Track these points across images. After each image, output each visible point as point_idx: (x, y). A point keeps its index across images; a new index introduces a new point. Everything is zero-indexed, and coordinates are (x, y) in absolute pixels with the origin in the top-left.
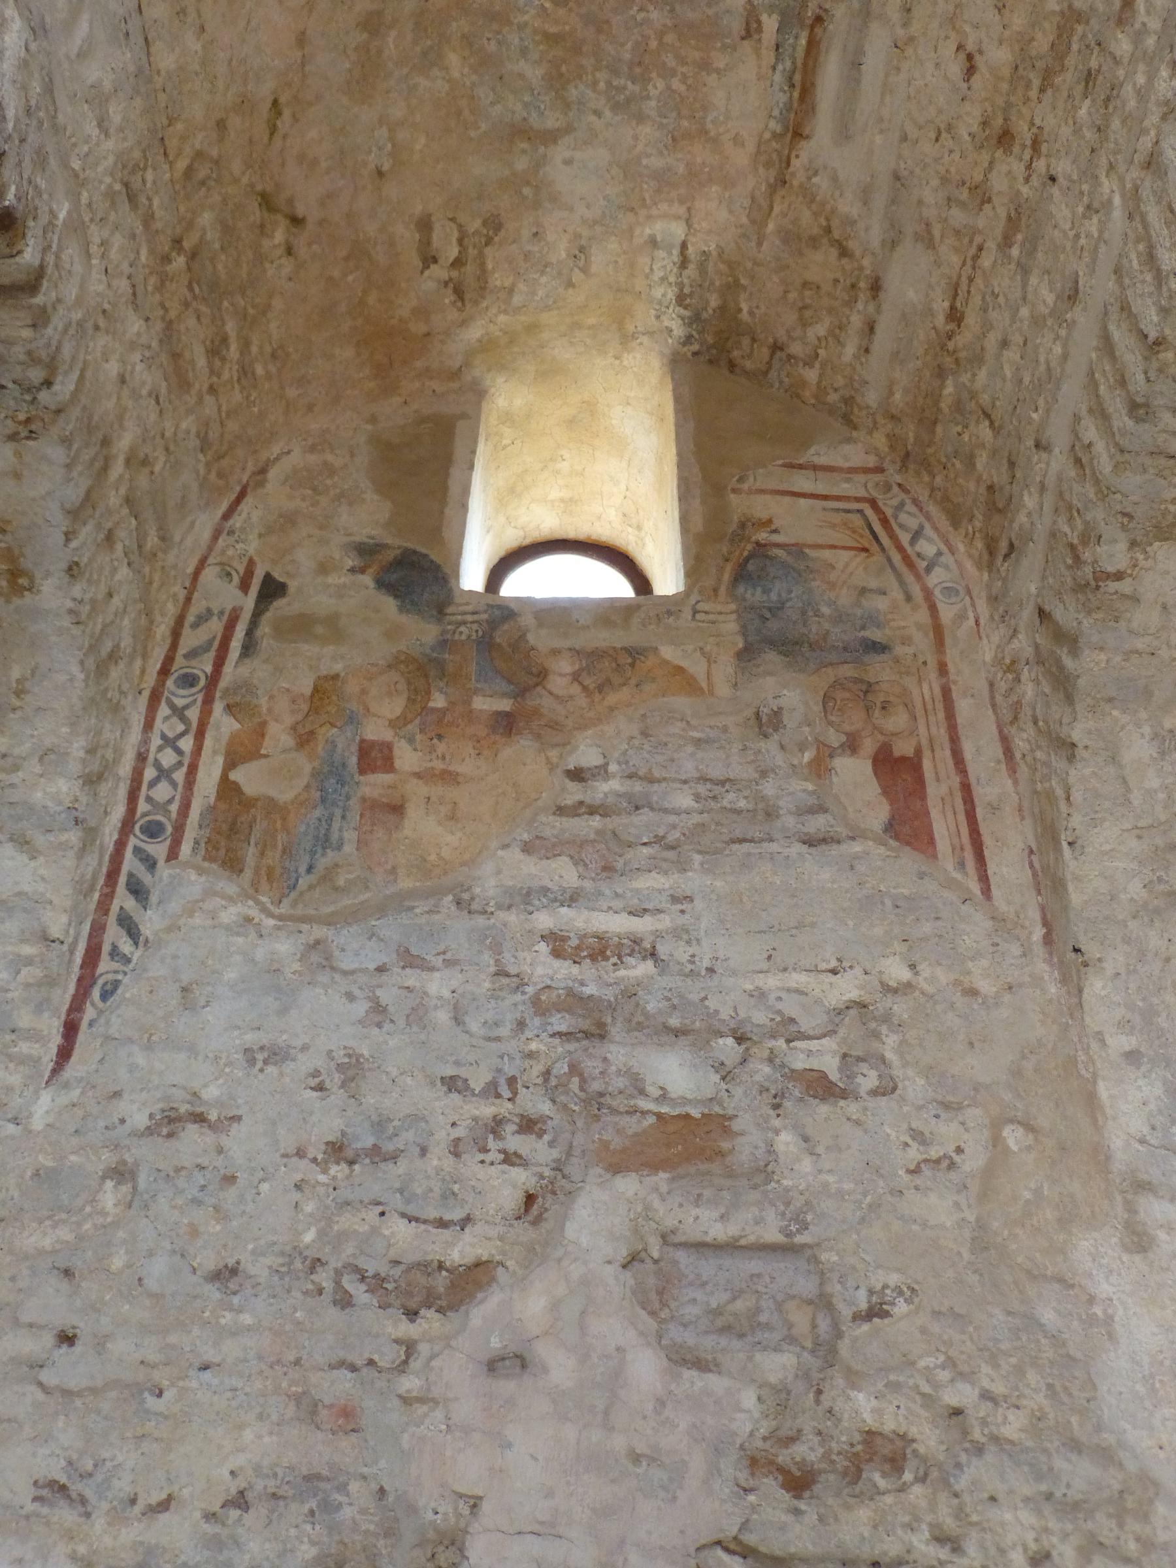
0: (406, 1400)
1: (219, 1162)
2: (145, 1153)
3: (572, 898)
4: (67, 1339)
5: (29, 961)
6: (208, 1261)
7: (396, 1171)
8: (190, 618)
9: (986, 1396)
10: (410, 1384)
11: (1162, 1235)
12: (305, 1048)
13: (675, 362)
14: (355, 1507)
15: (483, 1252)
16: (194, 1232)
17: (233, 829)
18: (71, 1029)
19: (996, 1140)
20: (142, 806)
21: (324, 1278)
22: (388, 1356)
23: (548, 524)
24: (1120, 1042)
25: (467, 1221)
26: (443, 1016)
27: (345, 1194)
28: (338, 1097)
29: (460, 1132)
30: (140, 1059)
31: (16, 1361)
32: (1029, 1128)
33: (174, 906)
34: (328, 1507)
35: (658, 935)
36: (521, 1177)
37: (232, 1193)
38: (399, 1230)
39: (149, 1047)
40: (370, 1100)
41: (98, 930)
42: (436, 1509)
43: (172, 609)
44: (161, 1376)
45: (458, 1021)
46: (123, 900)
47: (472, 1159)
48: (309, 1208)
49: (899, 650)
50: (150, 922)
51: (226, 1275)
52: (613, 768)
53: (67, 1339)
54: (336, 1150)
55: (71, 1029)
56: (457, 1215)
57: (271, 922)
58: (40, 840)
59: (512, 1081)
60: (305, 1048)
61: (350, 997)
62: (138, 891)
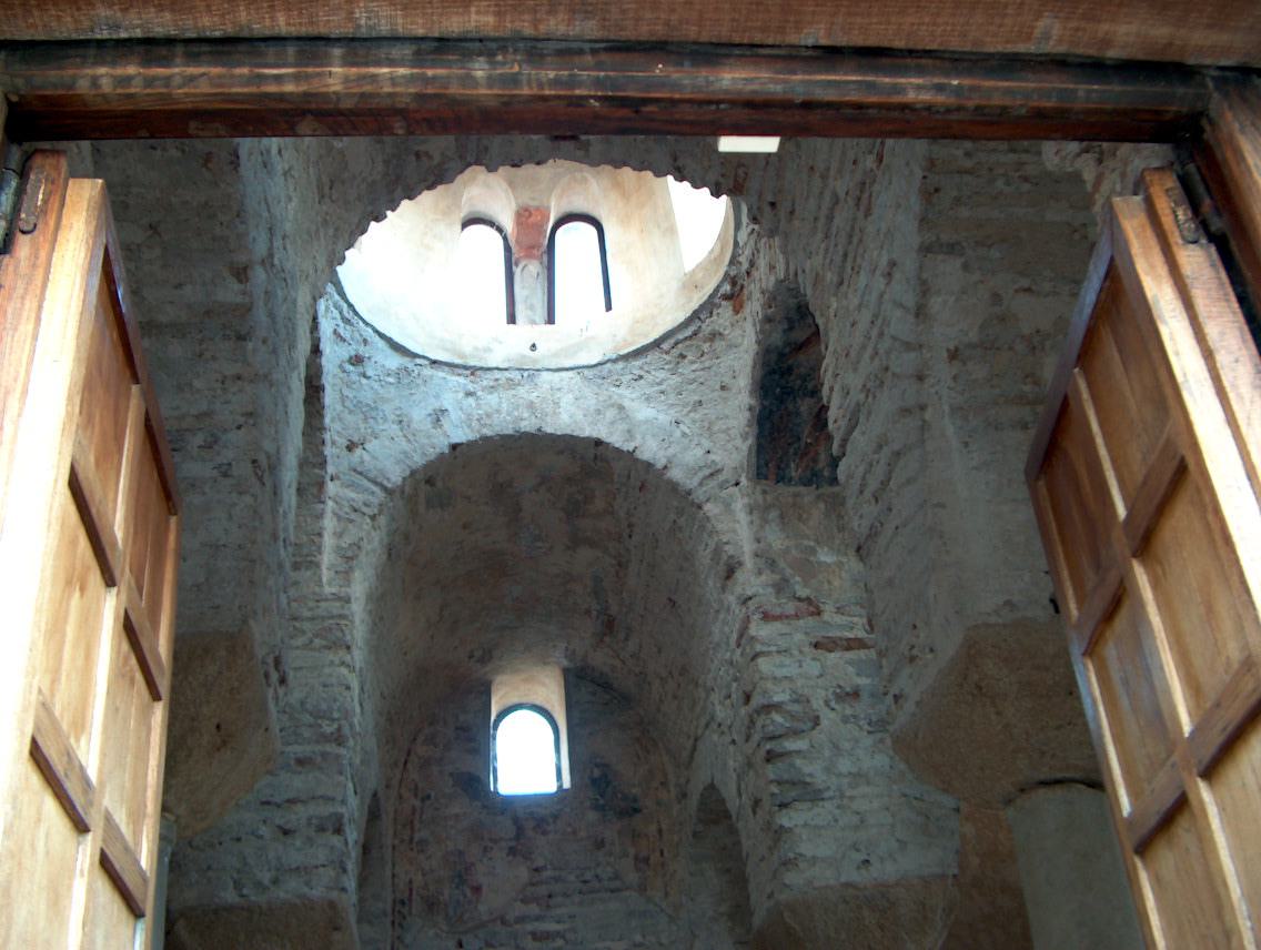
3: (538, 918)
13: (566, 672)
23: (515, 700)
35: (565, 931)
49: (645, 811)
52: (549, 867)
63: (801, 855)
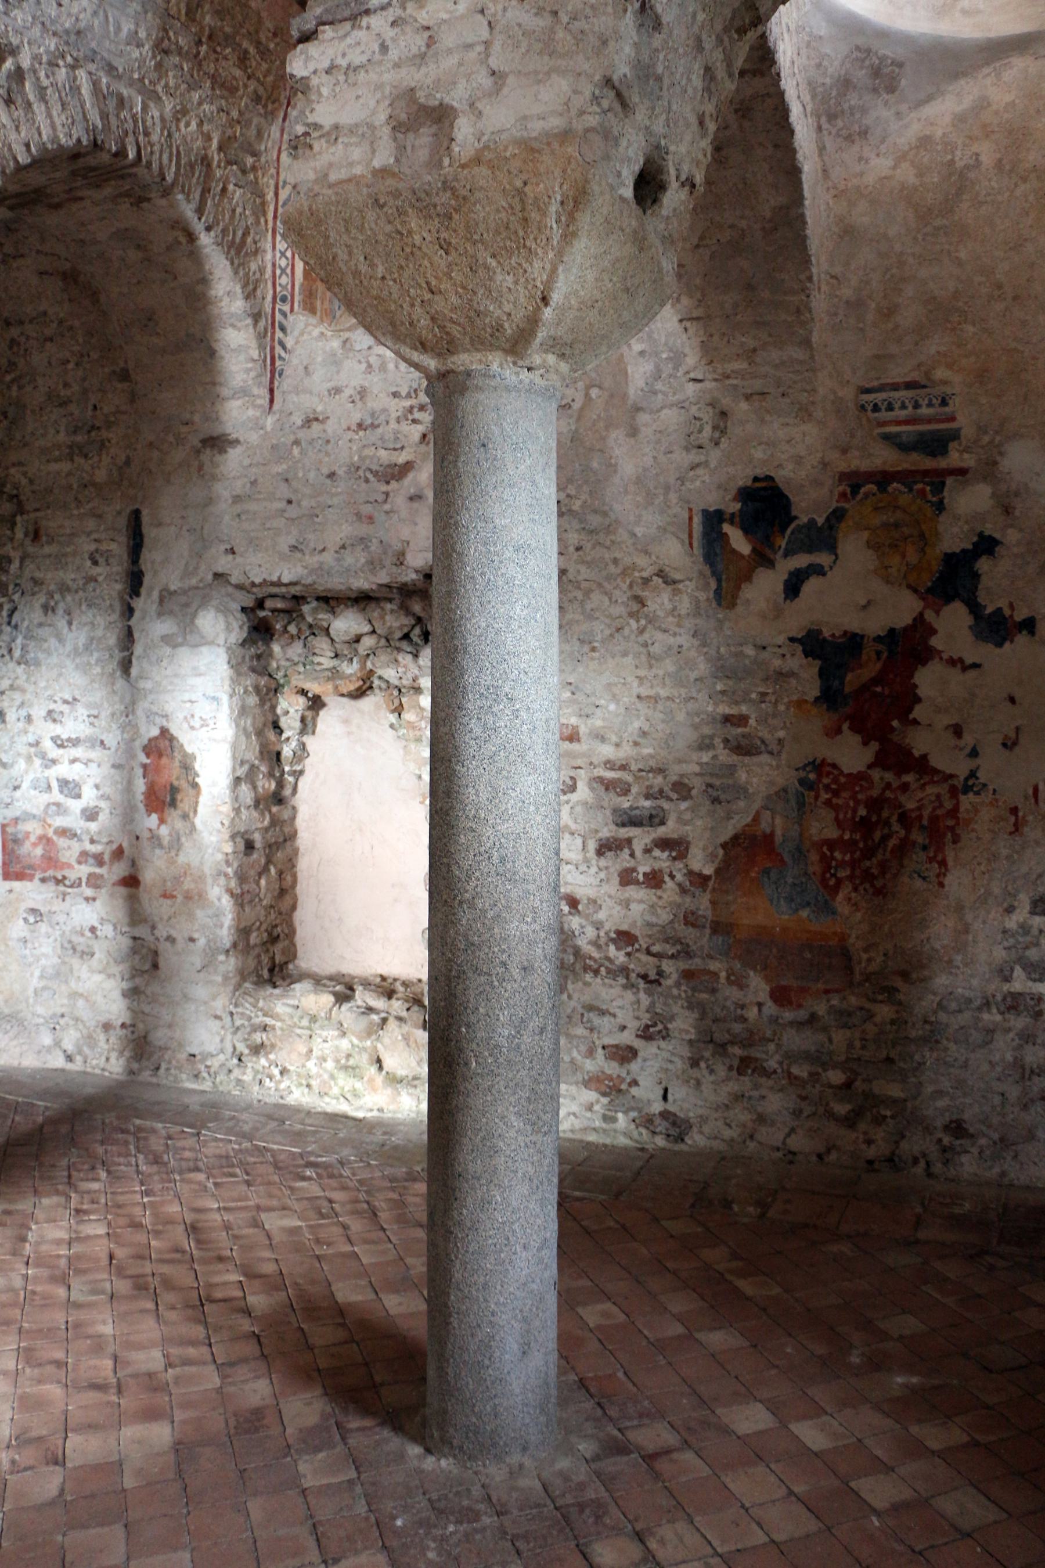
0: (387, 513)
2: (301, 435)
4: (290, 502)
5: (251, 369)
6: (325, 471)
7: (380, 430)
8: (281, 184)
9: (568, 496)
10: (387, 507)
11: (643, 429)
14: (374, 546)
15: (409, 458)
16: (321, 462)
17: (311, 294)
18: (271, 391)
20: (278, 289)
21: (361, 473)
22: (381, 498)
25: (402, 448)
27: (364, 442)
28: (359, 404)
31: (277, 510)
32: (600, 387)
33: (296, 333)
34: (367, 547)
36: (420, 429)
37: (330, 447)
38: (382, 453)
39: (297, 394)
41: (272, 349)
42: (397, 546)
43: (272, 182)
44: (317, 511)
46: (279, 334)
47: (404, 423)
50: (289, 342)
51: (332, 475)
53: (290, 502)
54: (360, 426)
55: (271, 391)
56: (398, 446)
58: (239, 324)
59: (416, 391)
61: (360, 362)
62: (283, 329)
63: (316, 126)
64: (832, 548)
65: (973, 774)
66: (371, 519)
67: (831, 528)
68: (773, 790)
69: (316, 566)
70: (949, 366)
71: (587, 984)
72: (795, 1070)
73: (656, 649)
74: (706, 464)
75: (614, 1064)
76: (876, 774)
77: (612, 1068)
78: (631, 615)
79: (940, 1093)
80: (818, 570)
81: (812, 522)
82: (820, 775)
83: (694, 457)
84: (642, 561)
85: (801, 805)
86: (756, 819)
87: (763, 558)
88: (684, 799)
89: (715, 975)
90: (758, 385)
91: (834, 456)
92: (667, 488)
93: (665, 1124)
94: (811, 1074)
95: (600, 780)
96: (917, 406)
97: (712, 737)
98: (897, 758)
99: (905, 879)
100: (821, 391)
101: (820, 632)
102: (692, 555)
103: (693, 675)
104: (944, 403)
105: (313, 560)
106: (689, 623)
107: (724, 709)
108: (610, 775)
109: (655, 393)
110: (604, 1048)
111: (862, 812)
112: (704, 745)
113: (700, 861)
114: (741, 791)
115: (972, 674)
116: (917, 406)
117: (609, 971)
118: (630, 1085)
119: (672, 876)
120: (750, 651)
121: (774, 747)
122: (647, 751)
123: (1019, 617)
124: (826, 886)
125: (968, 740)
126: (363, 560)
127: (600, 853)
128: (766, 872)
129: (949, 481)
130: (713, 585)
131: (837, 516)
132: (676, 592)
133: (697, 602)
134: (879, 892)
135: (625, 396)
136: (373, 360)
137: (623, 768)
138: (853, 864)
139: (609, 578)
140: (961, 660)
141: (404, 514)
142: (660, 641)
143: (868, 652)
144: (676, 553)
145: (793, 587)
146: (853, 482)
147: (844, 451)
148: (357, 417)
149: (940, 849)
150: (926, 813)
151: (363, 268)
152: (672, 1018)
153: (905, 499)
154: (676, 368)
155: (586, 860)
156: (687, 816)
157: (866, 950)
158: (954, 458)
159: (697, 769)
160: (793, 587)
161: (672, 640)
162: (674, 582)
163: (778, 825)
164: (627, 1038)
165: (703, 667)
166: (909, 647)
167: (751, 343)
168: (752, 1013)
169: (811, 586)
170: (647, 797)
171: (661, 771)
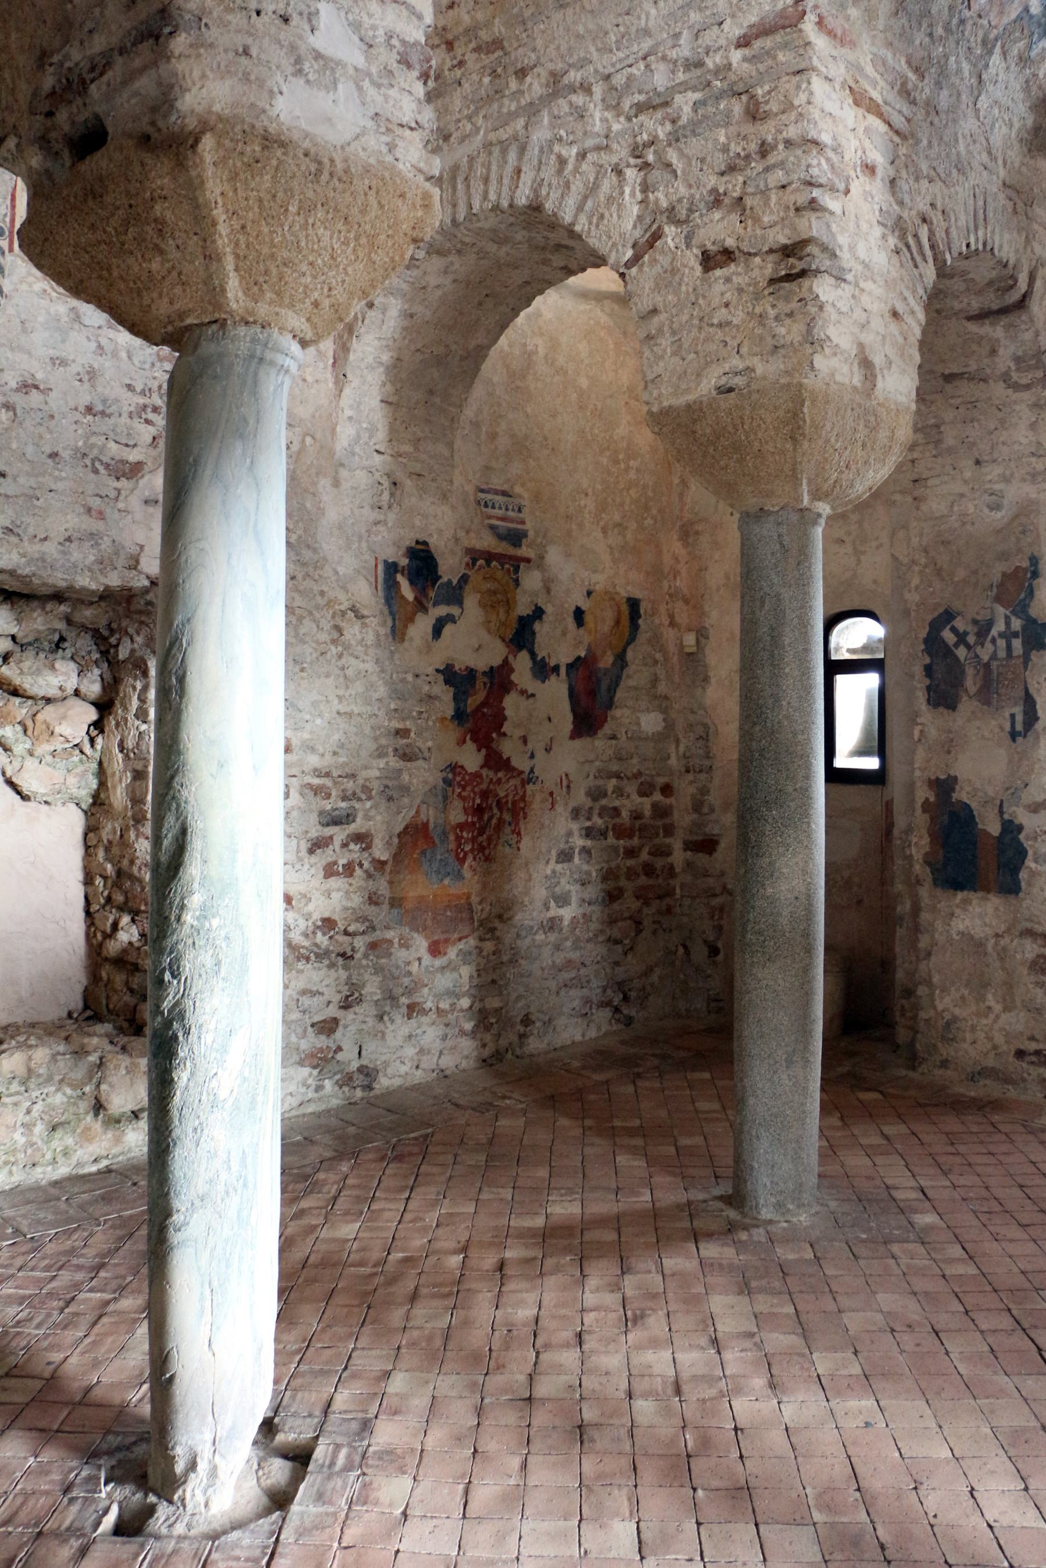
1: (46, 408)
2: (18, 399)
7: (112, 421)
12: (74, 361)
14: (106, 544)
16: (41, 437)
19: (303, 441)
22: (113, 494)
24: (348, 413)
25: (135, 445)
26: (123, 355)
27: (94, 429)
28: (87, 385)
29: (132, 409)
30: (9, 355)
34: (97, 544)
36: (152, 430)
37: (53, 423)
38: (112, 445)
39: (12, 349)
40: (100, 389)
44: (38, 493)
45: (129, 358)
47: (136, 420)
48: (80, 432)
51: (54, 455)
54: (89, 409)
56: (131, 443)
57: (54, 294)
60: (74, 361)
64: (459, 602)
65: (532, 771)
66: (101, 515)
67: (461, 588)
68: (427, 788)
69: (37, 556)
70: (523, 485)
71: (301, 971)
72: (442, 1005)
73: (349, 672)
74: (385, 523)
75: (323, 1037)
76: (485, 772)
77: (322, 1041)
78: (334, 642)
79: (519, 998)
80: (450, 619)
81: (450, 582)
82: (455, 775)
83: (376, 515)
84: (342, 596)
85: (445, 798)
86: (418, 812)
87: (420, 606)
88: (369, 798)
89: (390, 942)
90: (418, 467)
91: (461, 534)
92: (360, 538)
93: (361, 1077)
94: (451, 1005)
95: (309, 786)
96: (507, 509)
97: (387, 747)
98: (496, 761)
99: (500, 847)
100: (456, 483)
101: (453, 666)
102: (377, 596)
103: (376, 696)
104: (520, 511)
105: (34, 549)
106: (372, 651)
107: (396, 724)
108: (316, 781)
109: (353, 454)
110: (313, 1025)
111: (478, 801)
112: (381, 754)
113: (380, 851)
114: (405, 789)
115: (531, 700)
116: (507, 509)
117: (317, 955)
118: (335, 1052)
119: (361, 865)
120: (410, 678)
121: (426, 754)
122: (342, 760)
123: (552, 664)
124: (458, 859)
125: (530, 745)
126: (92, 558)
127: (311, 851)
128: (423, 853)
129: (522, 565)
130: (390, 623)
131: (464, 579)
132: (364, 625)
133: (378, 635)
134: (487, 859)
135: (332, 453)
136: (104, 341)
137: (327, 775)
138: (473, 840)
139: (318, 607)
140: (526, 691)
141: (138, 516)
142: (354, 665)
143: (479, 684)
144: (365, 592)
145: (437, 631)
146: (474, 556)
147: (468, 532)
148: (85, 399)
149: (517, 824)
150: (510, 798)
151: (833, 440)
152: (364, 985)
153: (499, 574)
154: (370, 438)
155: (300, 859)
156: (373, 813)
157: (480, 903)
158: (524, 551)
159: (377, 773)
160: (437, 631)
161: (362, 666)
162: (363, 617)
163: (430, 815)
164: (333, 1011)
165: (382, 691)
166: (500, 680)
167: (420, 434)
168: (414, 968)
169: (448, 630)
170: (344, 798)
171: (353, 776)
